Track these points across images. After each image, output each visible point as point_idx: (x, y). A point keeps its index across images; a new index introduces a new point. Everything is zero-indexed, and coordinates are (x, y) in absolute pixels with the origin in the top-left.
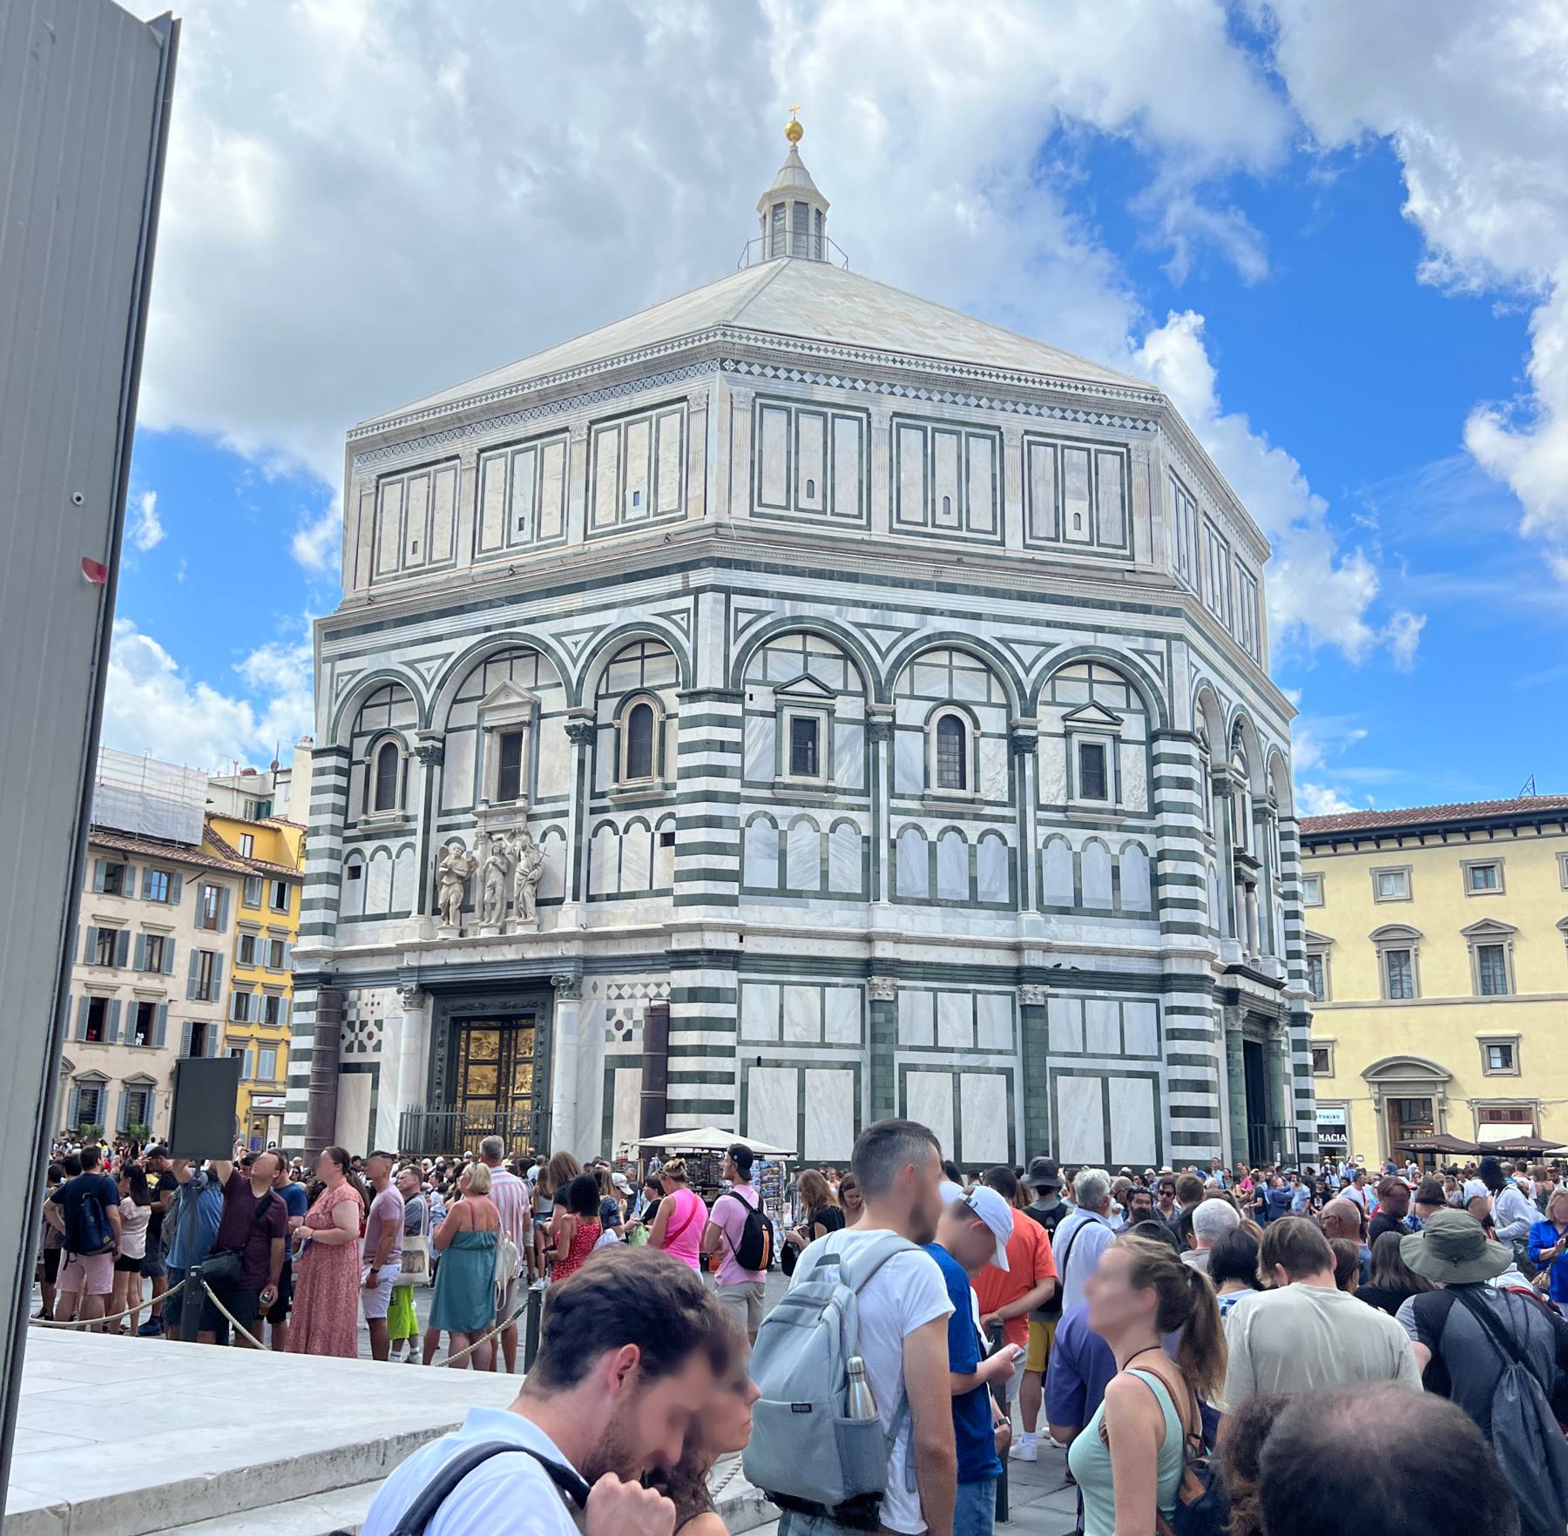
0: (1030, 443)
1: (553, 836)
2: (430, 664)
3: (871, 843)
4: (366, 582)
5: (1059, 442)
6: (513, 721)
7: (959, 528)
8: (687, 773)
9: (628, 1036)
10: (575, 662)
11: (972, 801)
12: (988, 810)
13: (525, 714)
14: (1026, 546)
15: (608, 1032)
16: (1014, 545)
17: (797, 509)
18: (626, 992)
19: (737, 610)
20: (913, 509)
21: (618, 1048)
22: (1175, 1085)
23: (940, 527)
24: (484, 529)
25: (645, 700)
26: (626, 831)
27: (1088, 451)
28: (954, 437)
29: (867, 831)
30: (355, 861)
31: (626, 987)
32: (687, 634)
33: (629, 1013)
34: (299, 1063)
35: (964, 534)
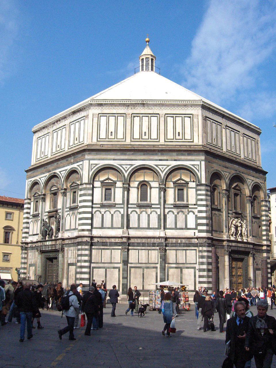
0: (167, 116)
3: (123, 216)
5: (174, 116)
7: (148, 139)
8: (81, 202)
11: (149, 204)
12: (153, 206)
14: (165, 141)
16: (162, 141)
17: (108, 139)
19: (91, 164)
20: (137, 136)
22: (200, 270)
23: (143, 139)
27: (182, 117)
28: (147, 118)
29: (122, 213)
35: (150, 140)
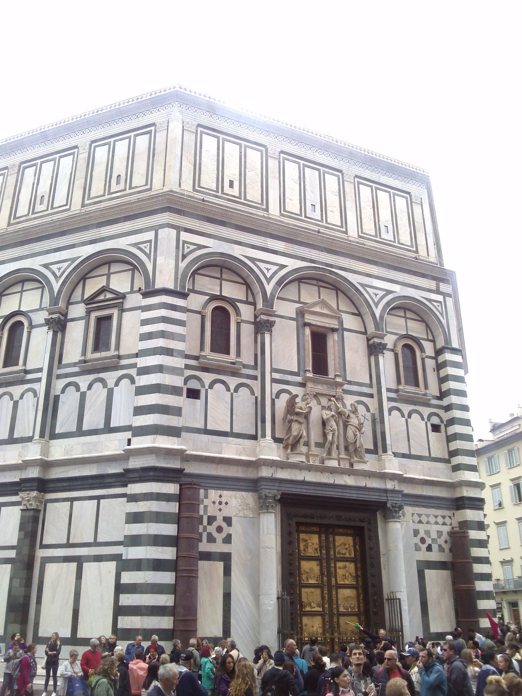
1: (361, 409)
2: (269, 266)
4: (190, 189)
6: (327, 326)
9: (429, 548)
10: (377, 305)
13: (334, 324)
15: (416, 544)
18: (424, 519)
21: (423, 556)
24: (287, 200)
25: (410, 342)
26: (410, 416)
30: (194, 384)
31: (424, 516)
32: (442, 314)
33: (427, 532)
34: (160, 549)
